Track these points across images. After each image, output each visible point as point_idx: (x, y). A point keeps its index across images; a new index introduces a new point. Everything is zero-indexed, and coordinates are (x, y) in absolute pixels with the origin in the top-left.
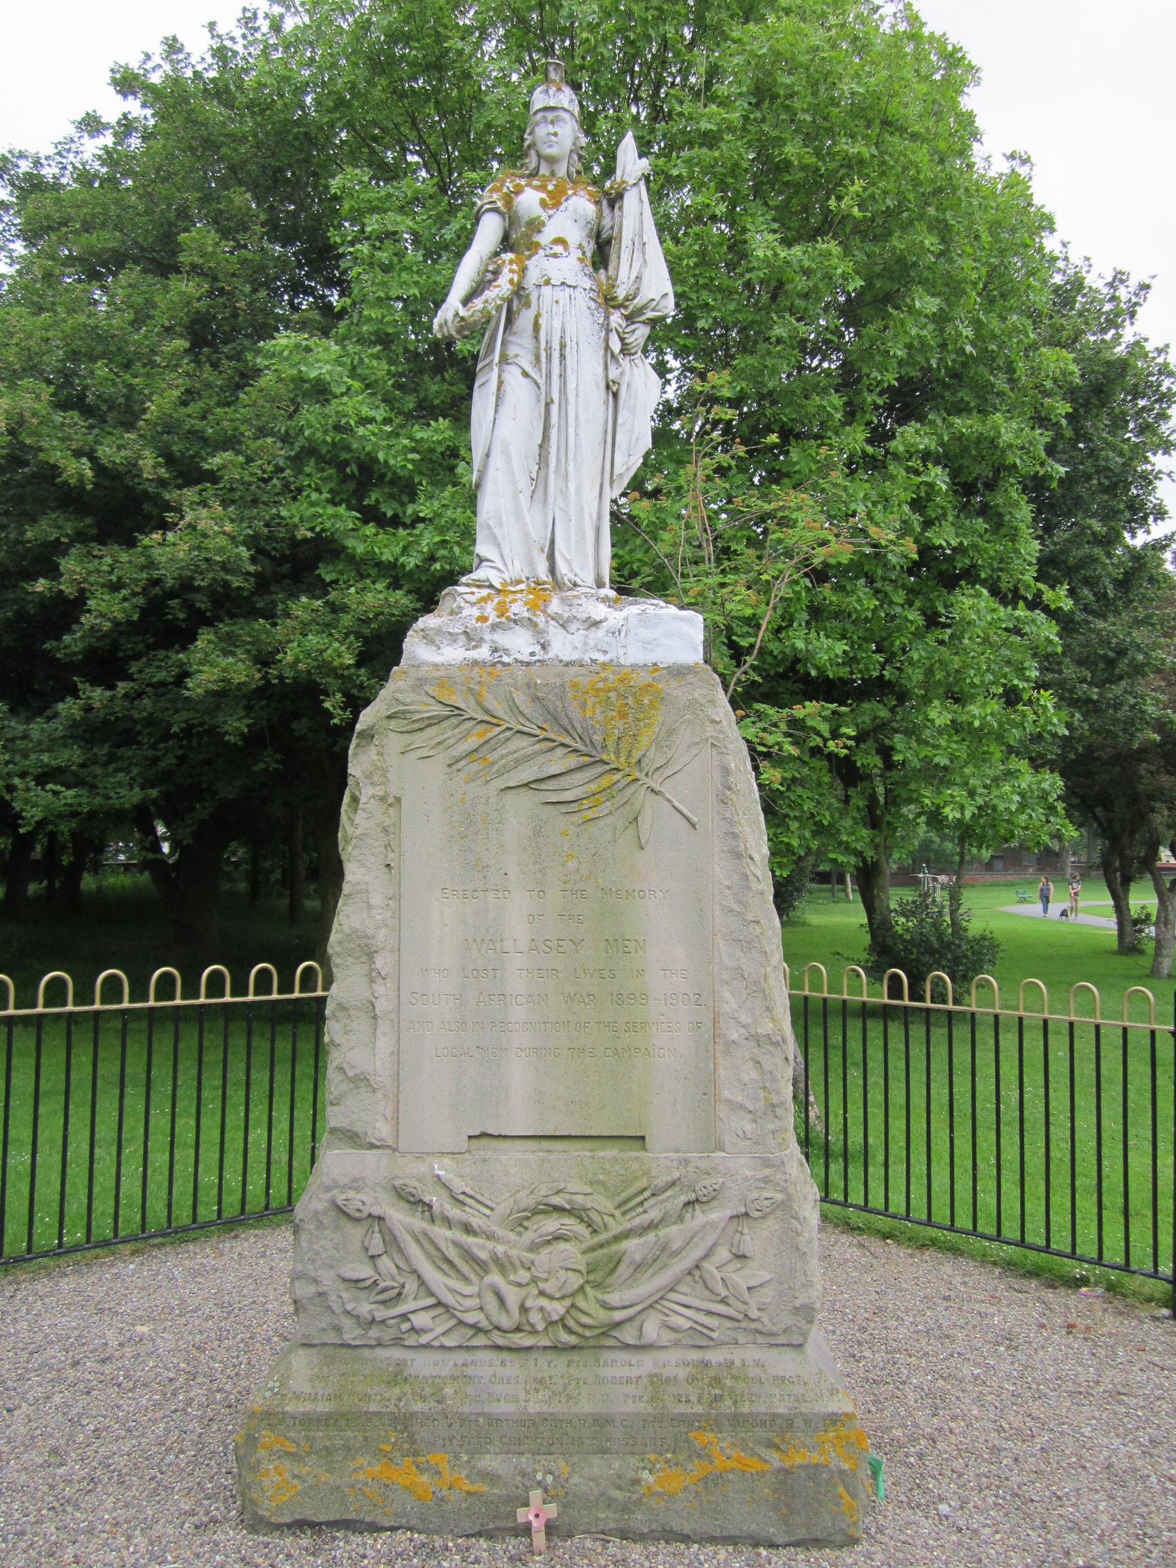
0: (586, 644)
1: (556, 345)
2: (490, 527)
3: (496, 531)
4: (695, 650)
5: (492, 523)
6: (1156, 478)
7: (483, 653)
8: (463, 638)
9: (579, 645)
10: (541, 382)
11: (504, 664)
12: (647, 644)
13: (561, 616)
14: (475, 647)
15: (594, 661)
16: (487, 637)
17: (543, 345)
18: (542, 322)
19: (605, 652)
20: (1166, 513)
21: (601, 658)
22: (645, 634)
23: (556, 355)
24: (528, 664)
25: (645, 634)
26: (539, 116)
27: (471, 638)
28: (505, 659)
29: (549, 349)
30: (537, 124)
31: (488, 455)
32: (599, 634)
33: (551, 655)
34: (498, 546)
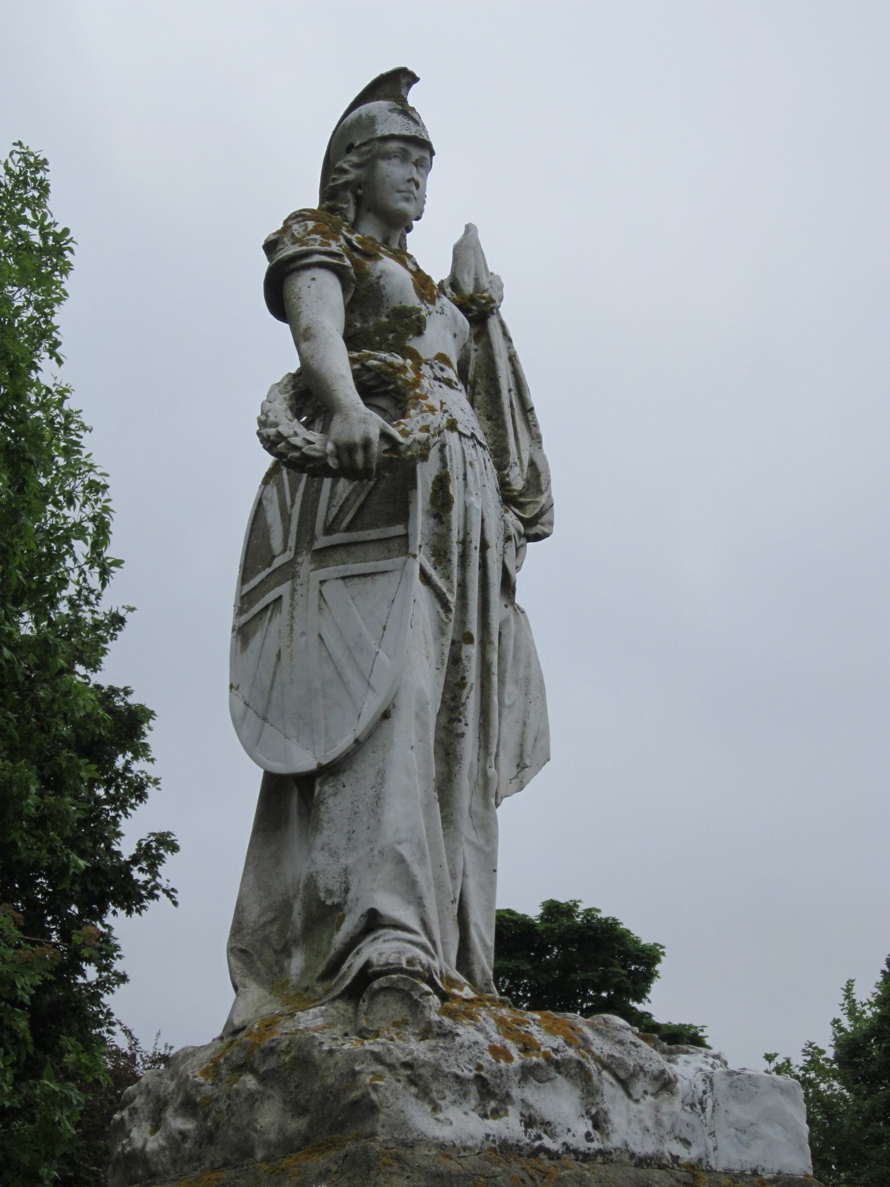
0: (659, 1123)
1: (476, 542)
2: (401, 860)
3: (415, 869)
4: (802, 1148)
5: (405, 851)
6: (152, 896)
7: (509, 1126)
8: (473, 1089)
9: (649, 1123)
10: (452, 599)
11: (552, 1155)
12: (744, 1131)
13: (622, 1064)
14: (496, 1114)
15: (675, 1159)
16: (515, 1092)
17: (455, 536)
18: (455, 488)
19: (687, 1143)
20: (117, 948)
21: (686, 1155)
22: (739, 1112)
23: (475, 556)
24: (585, 1157)
25: (739, 1112)
26: (394, 146)
27: (489, 1093)
28: (547, 1142)
29: (465, 543)
30: (387, 156)
31: (386, 715)
32: (673, 1106)
33: (615, 1141)
34: (419, 903)
